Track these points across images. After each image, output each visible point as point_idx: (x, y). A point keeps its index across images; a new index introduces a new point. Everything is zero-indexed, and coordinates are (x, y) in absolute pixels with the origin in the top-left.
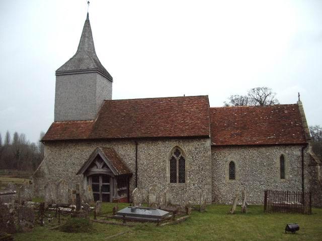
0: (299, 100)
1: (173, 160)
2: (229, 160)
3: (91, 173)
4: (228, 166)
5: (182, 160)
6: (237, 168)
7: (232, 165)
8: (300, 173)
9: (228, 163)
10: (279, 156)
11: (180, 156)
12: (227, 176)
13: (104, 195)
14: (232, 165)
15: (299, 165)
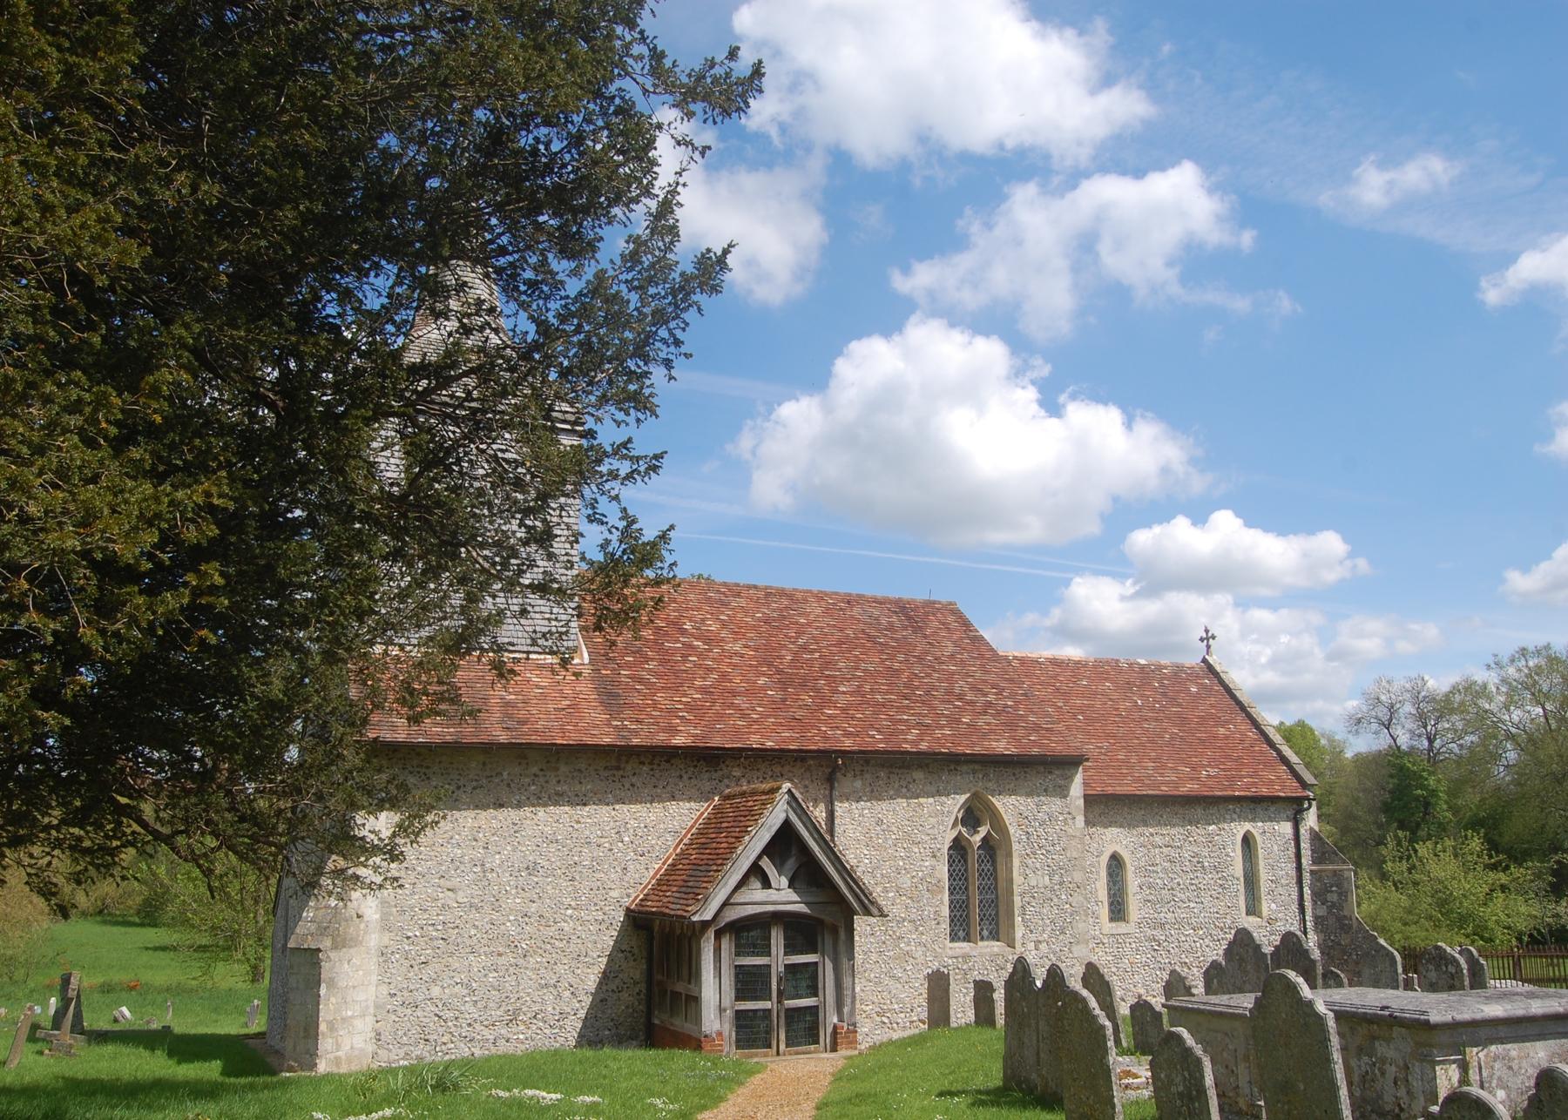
3: (732, 914)
6: (1133, 882)
9: (1105, 859)
12: (1104, 912)
13: (793, 1015)
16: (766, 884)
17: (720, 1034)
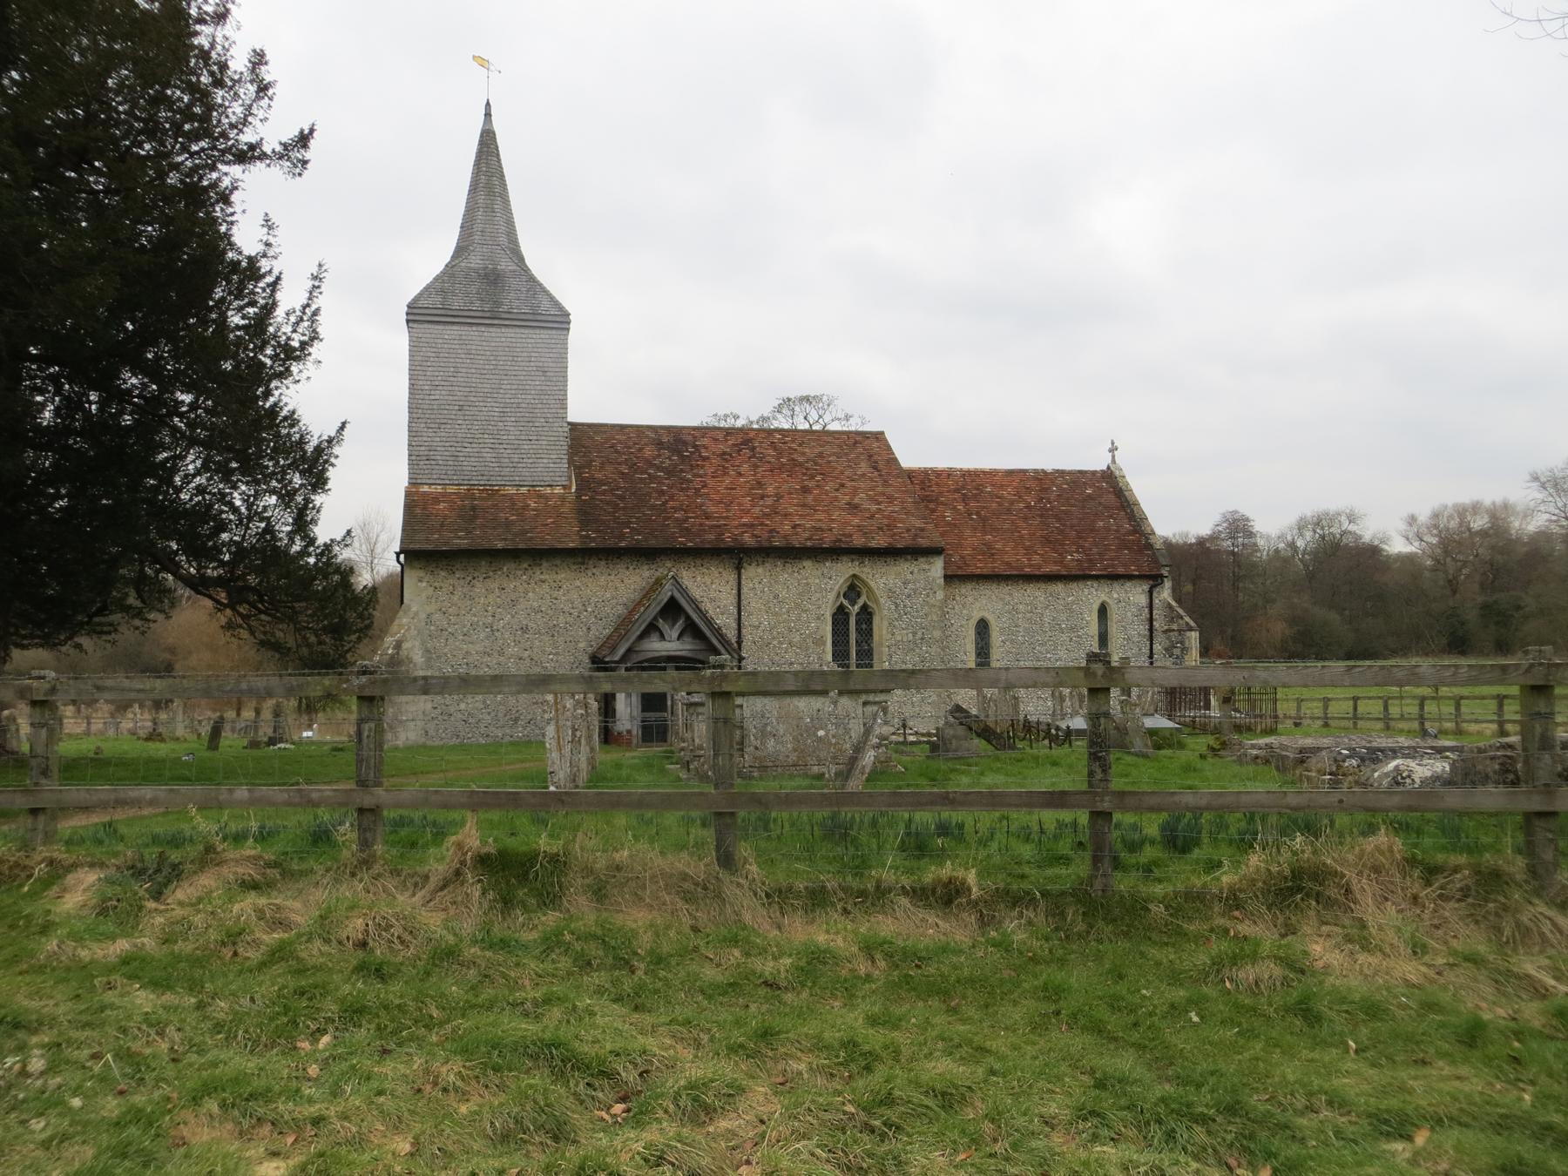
0: (1114, 461)
1: (840, 616)
2: (977, 616)
3: (636, 658)
4: (972, 633)
5: (866, 614)
7: (983, 628)
8: (1146, 650)
9: (973, 622)
10: (1096, 607)
11: (860, 602)
14: (983, 628)
15: (1143, 629)
16: (662, 637)
17: (629, 732)
